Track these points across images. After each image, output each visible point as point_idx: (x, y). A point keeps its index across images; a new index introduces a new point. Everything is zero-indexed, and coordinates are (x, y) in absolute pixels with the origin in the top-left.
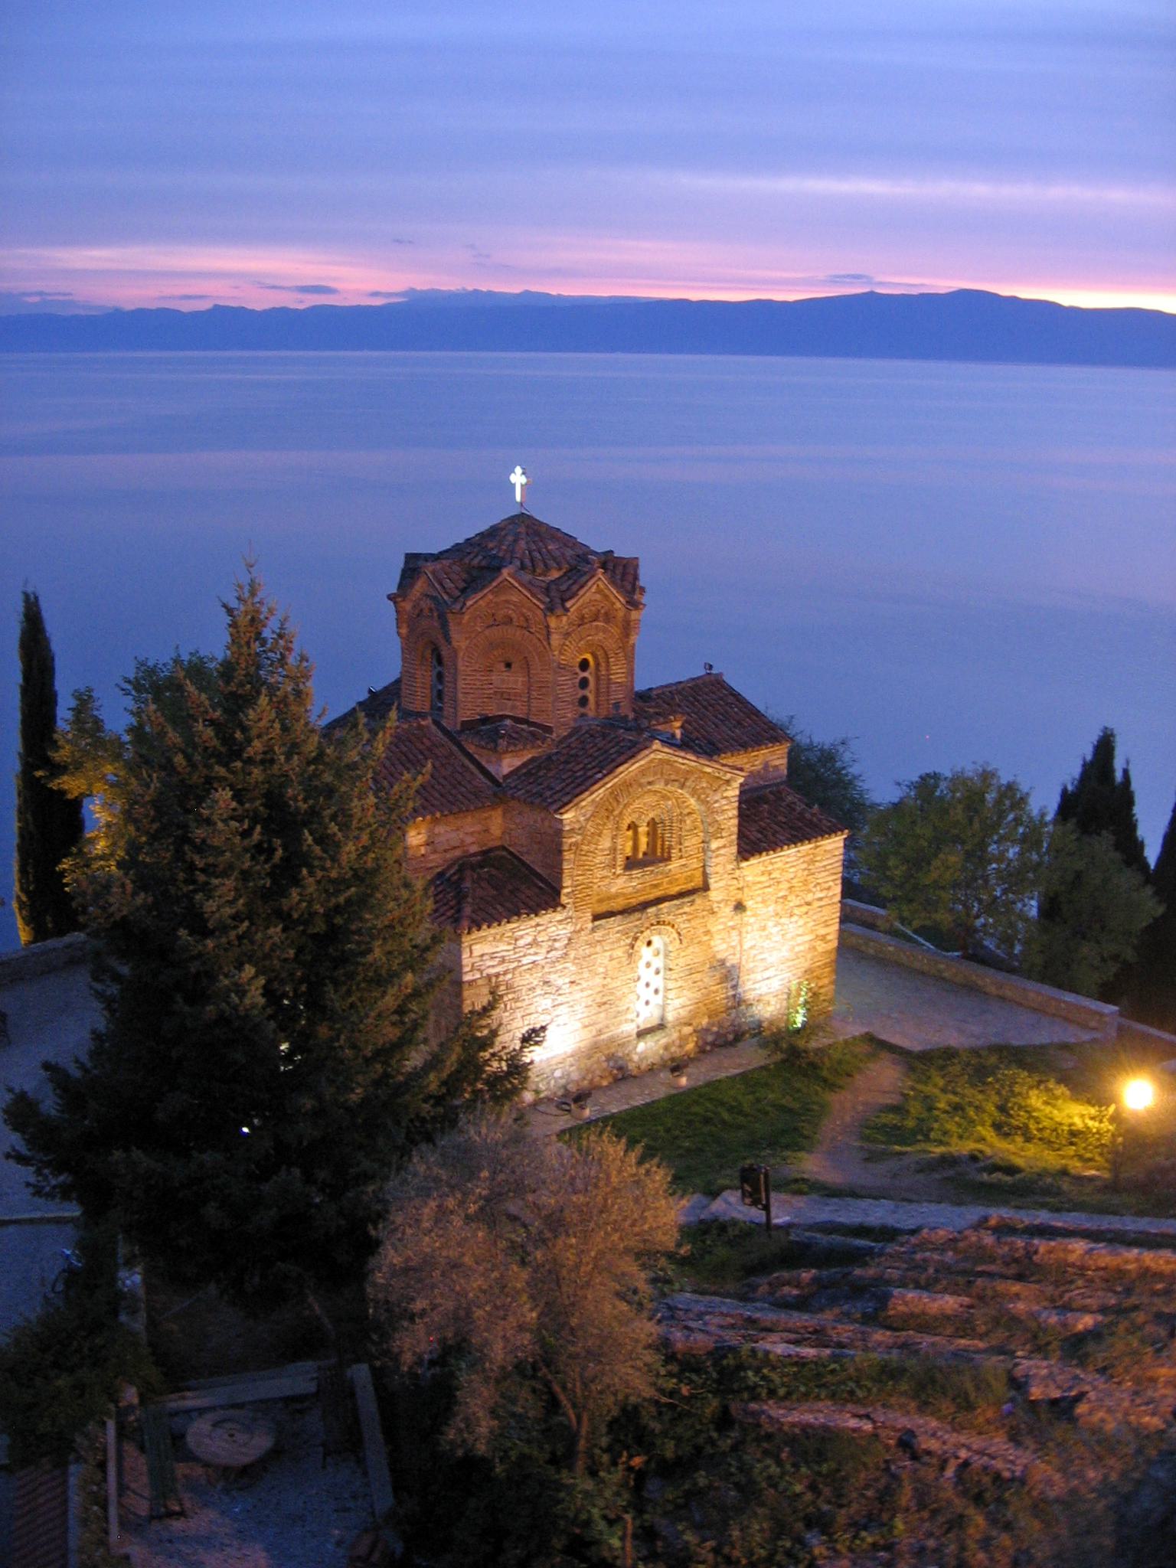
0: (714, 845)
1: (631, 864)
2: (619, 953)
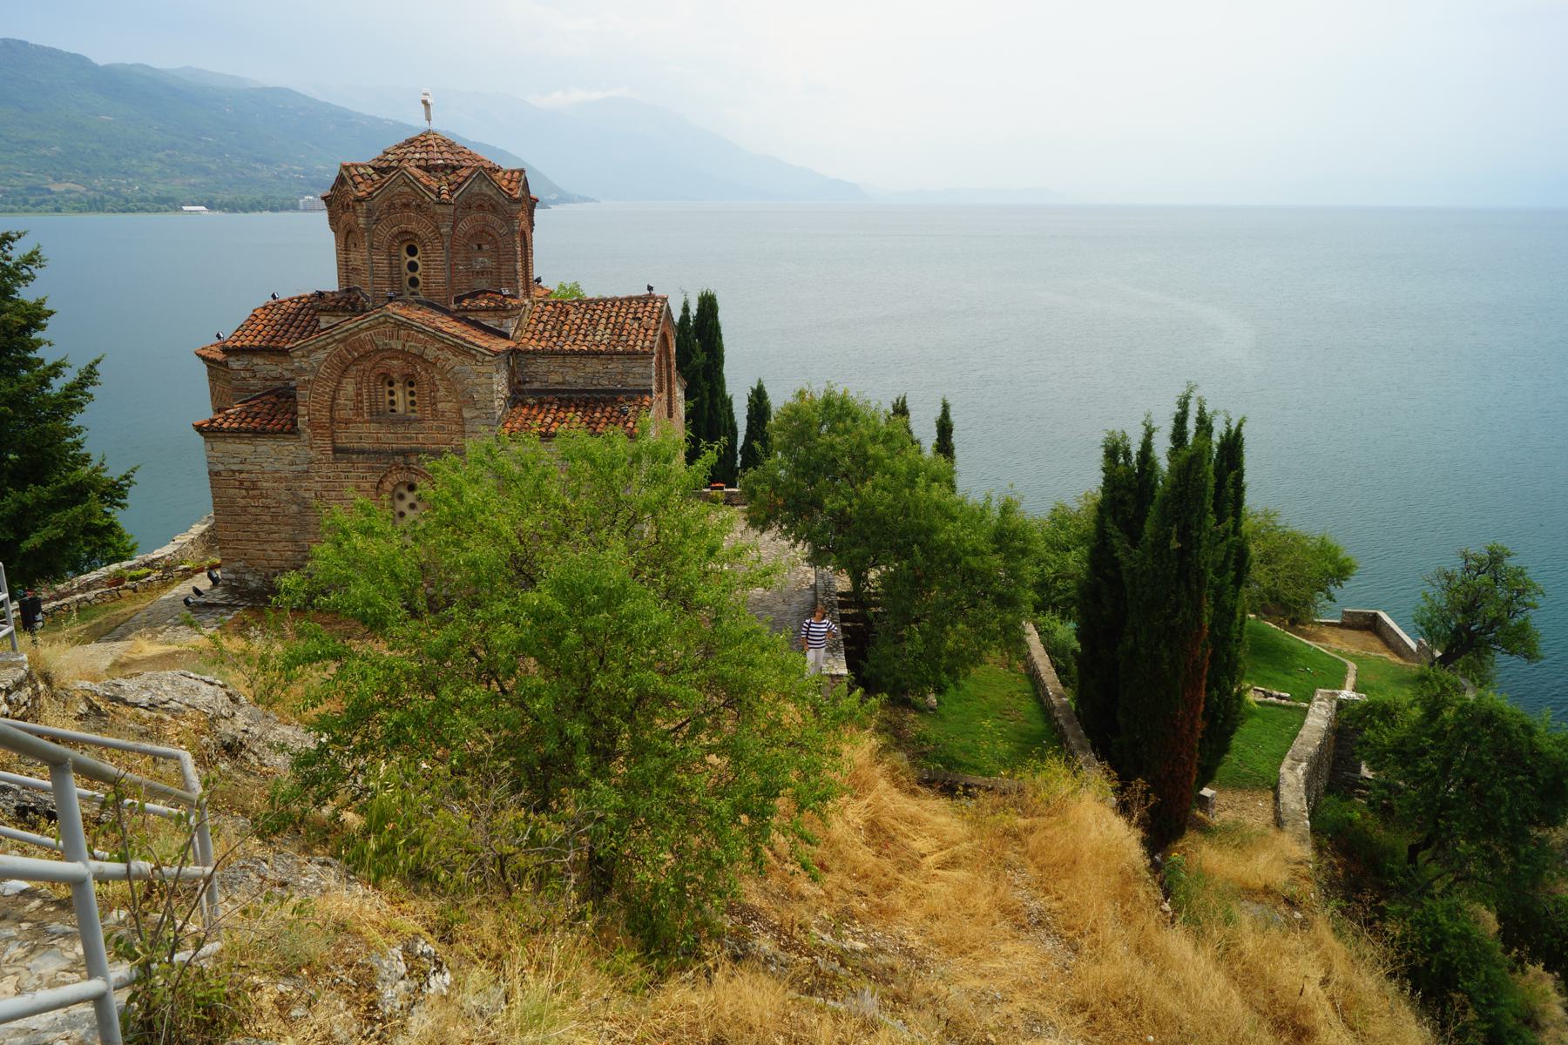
0: (467, 414)
2: (367, 485)
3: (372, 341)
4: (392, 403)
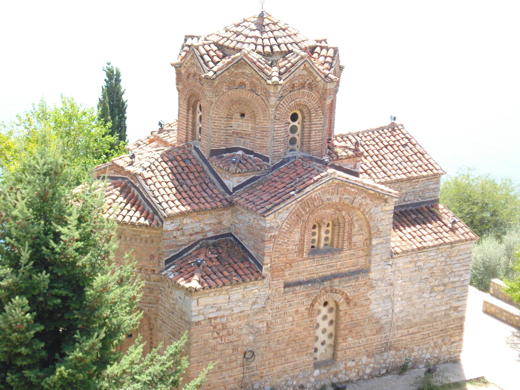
0: (374, 242)
1: (314, 251)
2: (302, 309)
3: (320, 198)
4: (313, 241)
